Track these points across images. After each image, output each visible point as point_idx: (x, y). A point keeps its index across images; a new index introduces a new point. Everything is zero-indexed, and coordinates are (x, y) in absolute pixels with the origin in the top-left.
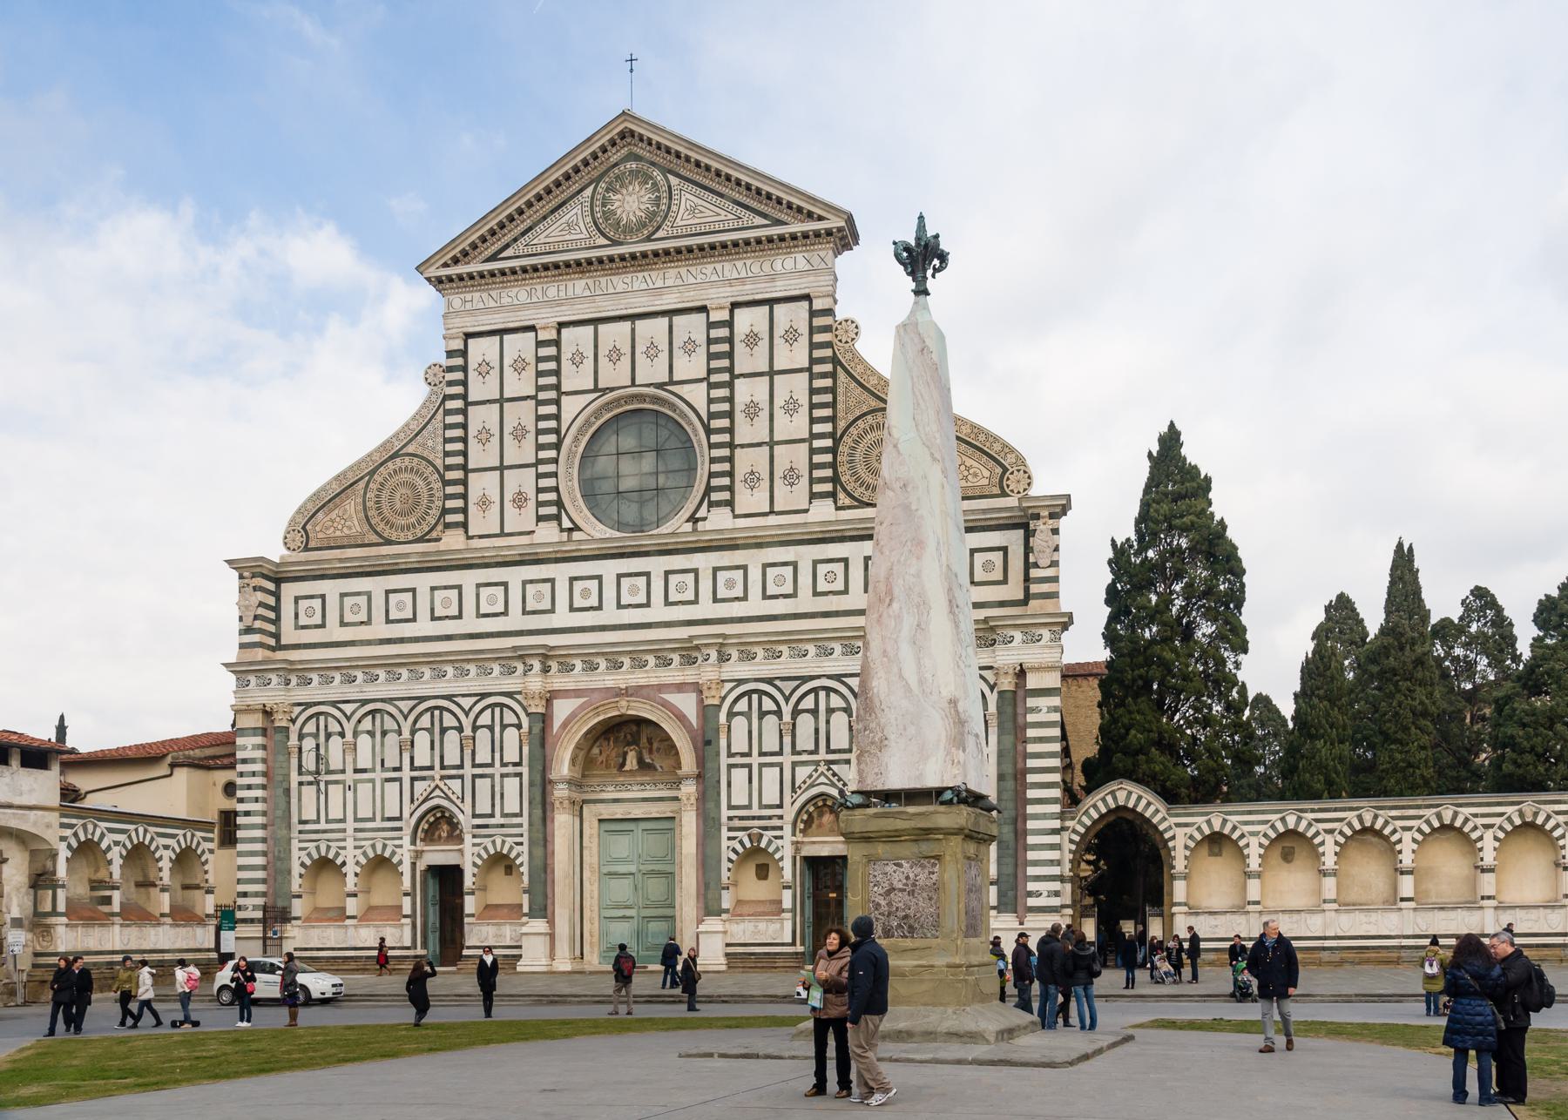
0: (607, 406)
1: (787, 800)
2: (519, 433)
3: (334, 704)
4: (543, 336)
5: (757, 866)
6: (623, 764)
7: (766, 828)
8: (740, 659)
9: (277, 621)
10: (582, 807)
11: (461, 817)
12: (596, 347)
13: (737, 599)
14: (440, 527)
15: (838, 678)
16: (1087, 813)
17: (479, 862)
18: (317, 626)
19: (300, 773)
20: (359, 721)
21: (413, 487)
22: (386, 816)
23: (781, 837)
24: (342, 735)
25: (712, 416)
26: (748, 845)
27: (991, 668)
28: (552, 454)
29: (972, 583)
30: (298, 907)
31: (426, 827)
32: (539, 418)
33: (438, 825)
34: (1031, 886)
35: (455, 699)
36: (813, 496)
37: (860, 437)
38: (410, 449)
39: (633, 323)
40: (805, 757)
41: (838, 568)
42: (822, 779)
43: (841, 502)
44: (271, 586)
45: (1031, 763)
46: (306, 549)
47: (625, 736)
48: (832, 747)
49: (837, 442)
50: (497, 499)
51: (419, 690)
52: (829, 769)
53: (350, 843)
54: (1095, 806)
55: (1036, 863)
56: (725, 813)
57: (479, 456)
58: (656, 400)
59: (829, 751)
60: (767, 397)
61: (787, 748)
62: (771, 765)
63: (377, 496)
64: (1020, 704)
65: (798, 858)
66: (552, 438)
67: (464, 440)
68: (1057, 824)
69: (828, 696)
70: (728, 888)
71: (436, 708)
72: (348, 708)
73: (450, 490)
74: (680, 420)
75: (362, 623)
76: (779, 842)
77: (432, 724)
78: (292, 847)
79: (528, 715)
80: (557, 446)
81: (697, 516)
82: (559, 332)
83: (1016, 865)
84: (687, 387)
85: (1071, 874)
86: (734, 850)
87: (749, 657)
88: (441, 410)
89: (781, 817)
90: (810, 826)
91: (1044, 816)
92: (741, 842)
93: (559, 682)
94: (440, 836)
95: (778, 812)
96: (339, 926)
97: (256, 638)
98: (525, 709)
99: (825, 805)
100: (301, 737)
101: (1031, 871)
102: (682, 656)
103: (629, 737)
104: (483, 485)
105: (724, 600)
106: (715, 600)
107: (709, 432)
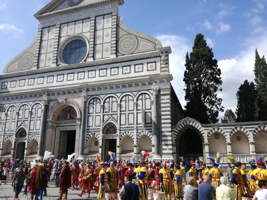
0: (69, 39)
2: (51, 46)
5: (95, 142)
6: (66, 117)
8: (92, 91)
13: (93, 77)
14: (33, 66)
16: (178, 127)
20: (9, 108)
21: (29, 58)
22: (11, 130)
29: (148, 71)
31: (20, 133)
32: (55, 42)
33: (21, 133)
36: (112, 54)
38: (29, 51)
39: (75, 22)
40: (106, 114)
42: (110, 119)
46: (7, 73)
48: (113, 111)
50: (45, 59)
52: (112, 116)
54: (181, 125)
59: (112, 112)
60: (102, 34)
61: (102, 111)
62: (98, 116)
68: (170, 129)
69: (112, 98)
75: (14, 87)
76: (99, 135)
77: (23, 108)
80: (58, 48)
82: (60, 26)
84: (85, 34)
91: (166, 127)
98: (43, 104)
102: (79, 90)
103: (68, 111)
105: (90, 78)
106: (88, 78)
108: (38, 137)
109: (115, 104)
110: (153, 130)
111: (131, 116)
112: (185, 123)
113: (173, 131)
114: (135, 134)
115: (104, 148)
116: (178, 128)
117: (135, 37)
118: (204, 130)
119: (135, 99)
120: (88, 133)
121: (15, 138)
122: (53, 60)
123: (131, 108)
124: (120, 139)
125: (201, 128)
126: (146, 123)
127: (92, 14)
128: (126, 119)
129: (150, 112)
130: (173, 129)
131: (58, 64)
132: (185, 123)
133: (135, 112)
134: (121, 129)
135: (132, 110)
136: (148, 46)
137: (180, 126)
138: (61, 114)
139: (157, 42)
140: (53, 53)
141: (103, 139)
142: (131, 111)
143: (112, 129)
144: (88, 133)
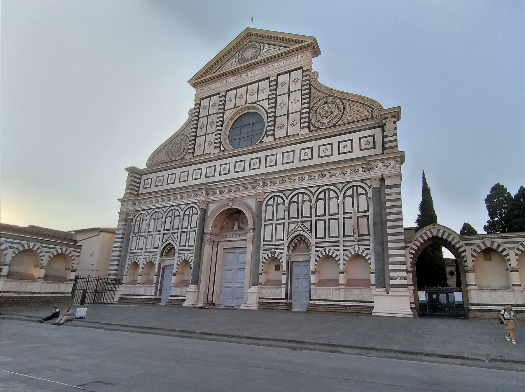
0: (238, 112)
1: (286, 237)
3: (146, 210)
4: (221, 95)
7: (277, 249)
8: (271, 185)
9: (138, 187)
10: (218, 244)
11: (176, 247)
12: (236, 96)
14: (187, 154)
15: (306, 188)
17: (179, 263)
18: (149, 187)
19: (134, 233)
20: (152, 215)
23: (283, 253)
24: (146, 220)
25: (269, 108)
26: (270, 256)
27: (369, 179)
28: (220, 128)
29: (361, 150)
30: (125, 280)
32: (218, 118)
34: (392, 274)
35: (180, 206)
36: (301, 128)
37: (318, 107)
38: (182, 134)
41: (309, 151)
43: (311, 129)
44: (139, 177)
45: (388, 217)
47: (235, 218)
49: (310, 110)
51: (170, 204)
52: (302, 225)
53: (142, 257)
54: (421, 237)
55: (393, 263)
56: (262, 243)
57: (200, 132)
58: (253, 107)
59: (303, 217)
61: (286, 217)
62: (280, 224)
63: (172, 148)
64: (382, 193)
65: (290, 261)
66: (221, 123)
67: (197, 128)
68: (403, 244)
69: (303, 196)
70: (262, 274)
71: (174, 209)
72: (149, 211)
73: (191, 143)
74: (260, 113)
75: (161, 185)
77: (172, 215)
78: (127, 259)
79: (200, 209)
80: (222, 126)
81: (263, 141)
83: (384, 264)
85: (412, 269)
86: (265, 258)
87: (274, 184)
88: (192, 121)
89: (283, 244)
90: (296, 249)
92: (268, 255)
93: (212, 198)
94: (171, 254)
95: (282, 242)
96: (135, 287)
97: (129, 191)
98: (199, 208)
99: (301, 239)
100: (136, 221)
101: (391, 267)
103: (236, 218)
104: (200, 140)
107: (267, 113)
108: (192, 256)
109: (307, 205)
110: (372, 246)
111: (334, 223)
112: (428, 233)
113: (408, 247)
114: (341, 252)
115: (289, 275)
116: (416, 242)
117: (339, 100)
118: (466, 244)
119: (341, 196)
120: (264, 252)
121: (159, 258)
122: (215, 143)
123: (334, 210)
124: (316, 260)
125: (458, 242)
126: (359, 236)
127: (271, 72)
128: (325, 228)
129: (365, 216)
130: (408, 245)
131: (222, 149)
132: (428, 233)
133: (341, 216)
134: (318, 245)
135: (336, 214)
136: (361, 112)
137: (420, 239)
138: (225, 223)
139: (375, 105)
140: (214, 134)
141: (288, 261)
142: (333, 215)
143: (303, 245)
144: (264, 252)
